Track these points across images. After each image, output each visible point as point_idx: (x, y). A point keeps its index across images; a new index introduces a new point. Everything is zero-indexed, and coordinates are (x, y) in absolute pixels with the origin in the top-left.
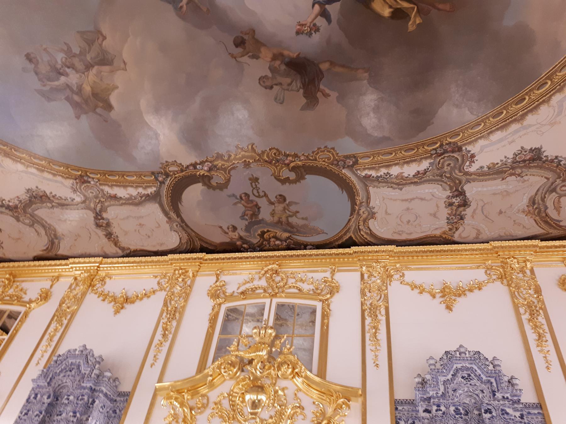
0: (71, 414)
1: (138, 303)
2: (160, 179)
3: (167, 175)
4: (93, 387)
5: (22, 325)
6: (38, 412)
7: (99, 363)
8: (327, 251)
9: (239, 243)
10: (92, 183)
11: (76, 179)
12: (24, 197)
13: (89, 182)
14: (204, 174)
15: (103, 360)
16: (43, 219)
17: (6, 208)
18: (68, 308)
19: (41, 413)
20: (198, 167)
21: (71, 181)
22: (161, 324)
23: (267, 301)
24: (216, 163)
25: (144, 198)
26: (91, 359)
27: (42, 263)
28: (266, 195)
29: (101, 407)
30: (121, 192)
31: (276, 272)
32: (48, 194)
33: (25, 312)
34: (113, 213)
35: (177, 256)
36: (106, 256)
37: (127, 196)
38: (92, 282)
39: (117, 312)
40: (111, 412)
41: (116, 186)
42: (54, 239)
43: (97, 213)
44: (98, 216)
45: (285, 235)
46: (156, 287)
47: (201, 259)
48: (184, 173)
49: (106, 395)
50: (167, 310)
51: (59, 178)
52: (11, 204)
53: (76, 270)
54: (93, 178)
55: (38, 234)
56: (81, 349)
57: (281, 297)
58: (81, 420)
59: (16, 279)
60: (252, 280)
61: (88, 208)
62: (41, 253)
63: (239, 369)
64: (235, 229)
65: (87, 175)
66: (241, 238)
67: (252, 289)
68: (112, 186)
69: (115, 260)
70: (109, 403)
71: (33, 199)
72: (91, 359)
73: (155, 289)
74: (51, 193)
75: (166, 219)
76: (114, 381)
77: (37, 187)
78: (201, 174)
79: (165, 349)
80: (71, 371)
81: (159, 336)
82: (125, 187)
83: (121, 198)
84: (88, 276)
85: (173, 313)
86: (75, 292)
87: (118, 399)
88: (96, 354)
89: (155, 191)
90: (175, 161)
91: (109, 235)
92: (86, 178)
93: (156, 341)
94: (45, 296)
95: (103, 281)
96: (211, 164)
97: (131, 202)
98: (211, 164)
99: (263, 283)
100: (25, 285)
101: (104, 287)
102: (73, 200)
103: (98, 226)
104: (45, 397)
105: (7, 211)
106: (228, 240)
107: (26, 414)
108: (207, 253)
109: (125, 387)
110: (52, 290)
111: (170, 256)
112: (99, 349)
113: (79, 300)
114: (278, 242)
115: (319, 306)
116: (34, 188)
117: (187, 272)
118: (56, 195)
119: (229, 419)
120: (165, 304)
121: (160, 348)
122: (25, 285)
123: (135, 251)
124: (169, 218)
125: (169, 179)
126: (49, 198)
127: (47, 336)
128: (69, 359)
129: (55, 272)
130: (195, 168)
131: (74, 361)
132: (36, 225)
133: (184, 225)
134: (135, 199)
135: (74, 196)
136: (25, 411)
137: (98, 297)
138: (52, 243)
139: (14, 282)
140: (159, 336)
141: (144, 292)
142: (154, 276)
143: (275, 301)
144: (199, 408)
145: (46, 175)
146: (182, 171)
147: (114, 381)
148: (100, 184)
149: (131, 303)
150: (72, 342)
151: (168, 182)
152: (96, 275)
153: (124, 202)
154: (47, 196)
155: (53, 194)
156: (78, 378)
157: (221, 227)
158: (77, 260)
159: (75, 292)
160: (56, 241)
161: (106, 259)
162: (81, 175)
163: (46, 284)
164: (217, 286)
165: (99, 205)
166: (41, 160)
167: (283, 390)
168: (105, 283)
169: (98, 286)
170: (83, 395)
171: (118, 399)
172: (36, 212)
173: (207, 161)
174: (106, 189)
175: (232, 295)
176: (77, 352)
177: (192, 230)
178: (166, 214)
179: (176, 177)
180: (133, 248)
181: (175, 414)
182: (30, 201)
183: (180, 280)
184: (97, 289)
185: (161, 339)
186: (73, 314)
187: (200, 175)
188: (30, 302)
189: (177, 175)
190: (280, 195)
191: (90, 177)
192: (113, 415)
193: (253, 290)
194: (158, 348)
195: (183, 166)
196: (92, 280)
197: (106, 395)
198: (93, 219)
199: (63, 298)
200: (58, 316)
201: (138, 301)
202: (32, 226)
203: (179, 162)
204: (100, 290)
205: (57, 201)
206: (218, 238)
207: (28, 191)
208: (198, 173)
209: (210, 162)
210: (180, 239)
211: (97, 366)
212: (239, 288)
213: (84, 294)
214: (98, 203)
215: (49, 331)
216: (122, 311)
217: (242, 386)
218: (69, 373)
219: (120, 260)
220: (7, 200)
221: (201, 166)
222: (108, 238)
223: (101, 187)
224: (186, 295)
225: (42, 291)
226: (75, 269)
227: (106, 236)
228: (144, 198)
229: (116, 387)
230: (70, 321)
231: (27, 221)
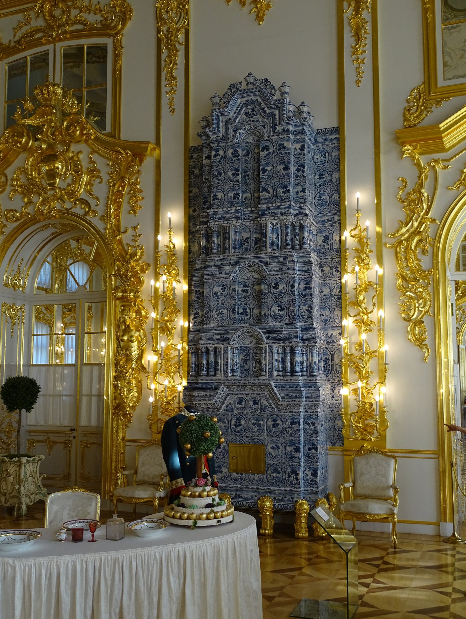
23: (50, 47)
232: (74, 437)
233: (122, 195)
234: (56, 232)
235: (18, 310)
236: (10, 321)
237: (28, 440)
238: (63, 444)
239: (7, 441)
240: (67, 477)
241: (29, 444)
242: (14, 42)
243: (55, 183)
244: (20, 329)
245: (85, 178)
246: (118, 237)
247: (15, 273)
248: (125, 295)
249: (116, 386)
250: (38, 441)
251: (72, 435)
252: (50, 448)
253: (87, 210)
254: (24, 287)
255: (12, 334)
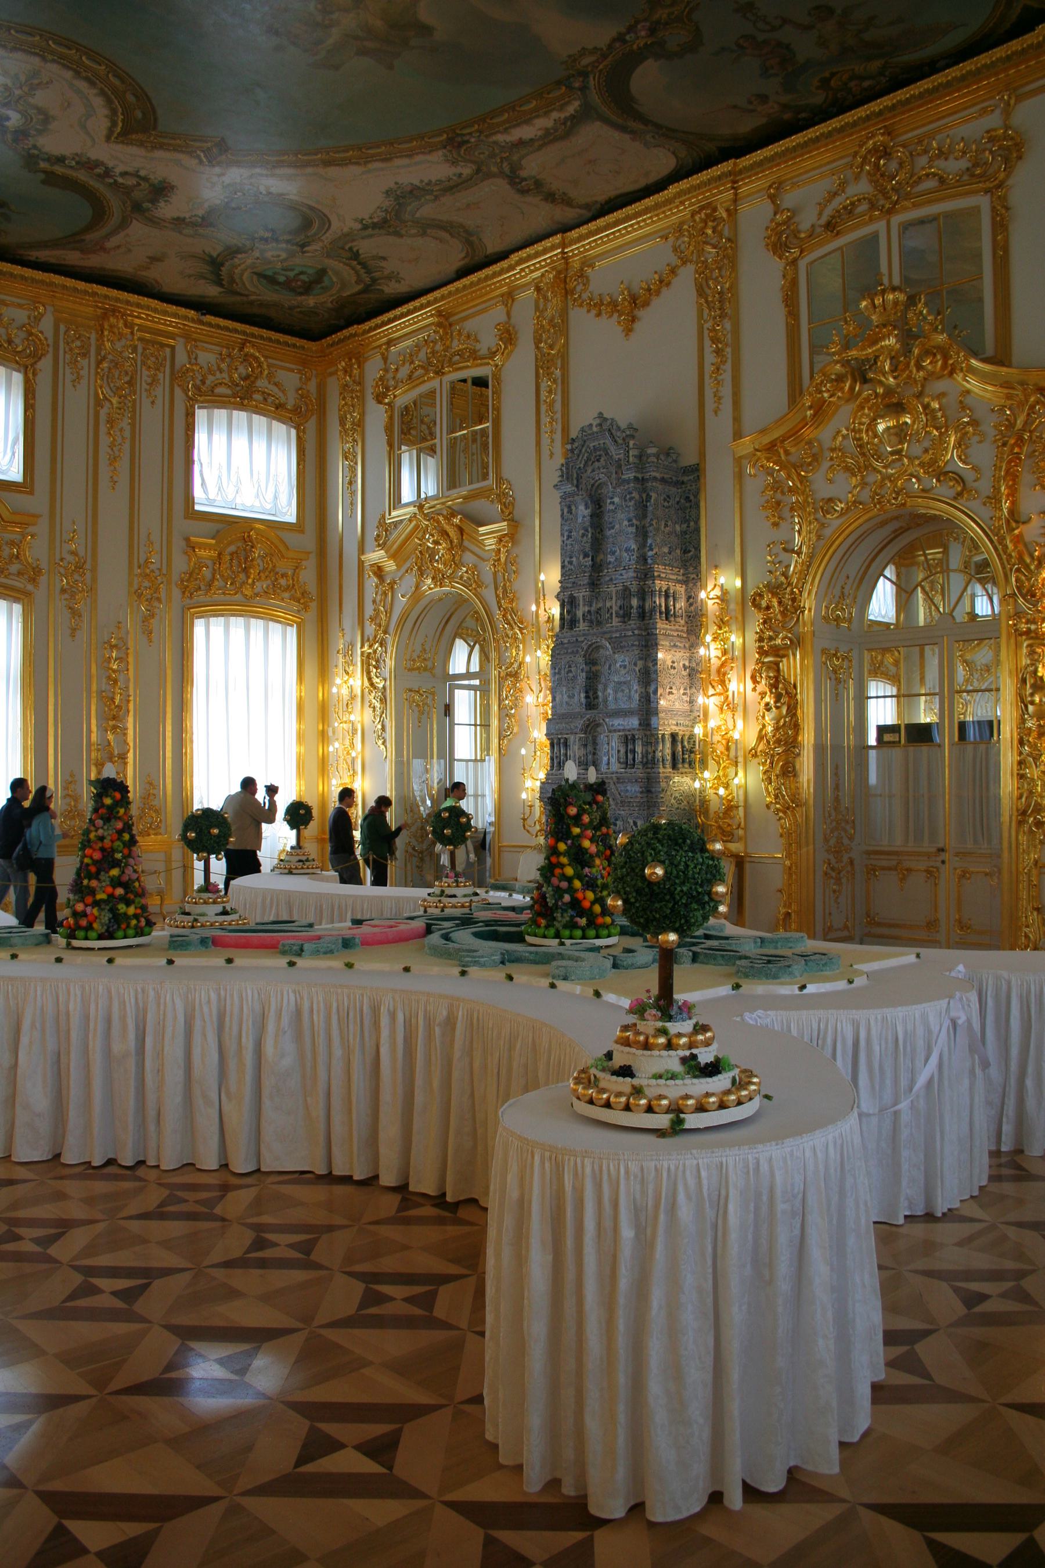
0: (626, 523)
1: (656, 302)
2: (577, 85)
3: (584, 74)
4: (640, 476)
5: (499, 397)
6: (582, 532)
7: (632, 437)
8: (983, 59)
9: (787, 116)
10: (473, 140)
11: (445, 148)
12: (387, 203)
13: (468, 142)
14: (646, 44)
15: (636, 430)
16: (433, 219)
17: (373, 228)
18: (551, 347)
19: (587, 531)
20: (628, 38)
21: (440, 153)
22: (706, 332)
23: (880, 226)
24: (656, 17)
25: (569, 123)
26: (619, 434)
27: (473, 278)
28: (785, 21)
29: (665, 500)
30: (526, 132)
31: (886, 153)
32: (418, 184)
33: (494, 375)
34: (532, 166)
35: (684, 184)
36: (566, 229)
37: (539, 133)
38: (566, 282)
39: (628, 331)
40: (682, 501)
41: (515, 126)
42: (468, 237)
43: (508, 176)
44: (514, 179)
45: (875, 65)
46: (675, 261)
47: (730, 173)
48: (610, 58)
49: (663, 480)
50: (707, 302)
51: (419, 158)
52: (375, 220)
53: (532, 272)
54: (470, 134)
55: (441, 241)
56: (598, 421)
57: (905, 209)
58: (644, 527)
59: (451, 319)
60: (843, 185)
61: (489, 175)
62: (462, 263)
63: (854, 381)
64: (763, 98)
65: (458, 135)
66: (785, 107)
67: (845, 208)
68: (506, 131)
69: (583, 230)
70: (674, 490)
71: (401, 201)
72: (619, 434)
73: (674, 265)
74: (422, 181)
75: (627, 137)
76: (668, 454)
77: (396, 183)
78: (641, 45)
79: (727, 376)
80: (598, 460)
81: (710, 358)
82: (528, 122)
83: (531, 140)
84: (555, 277)
85: (719, 304)
86: (549, 313)
87: (686, 479)
88: (623, 425)
89: (580, 106)
90: (583, 48)
91: (551, 197)
92: (459, 139)
93: (709, 369)
94: (508, 336)
95: (582, 276)
96: (648, 24)
97: (549, 138)
98: (648, 24)
99: (864, 187)
100: (470, 326)
101: (590, 289)
102: (460, 175)
103: (524, 192)
104: (582, 507)
105: (377, 231)
106: (764, 120)
107: (569, 537)
108: (737, 158)
109: (689, 459)
110: (513, 321)
111: (672, 190)
112: (623, 415)
113: (561, 326)
114: (866, 84)
115: (984, 202)
116: (392, 185)
117: (715, 210)
118: (430, 181)
119: (859, 471)
120: (701, 292)
121: (720, 378)
122: (470, 326)
123: (609, 201)
124: (632, 132)
125: (591, 78)
126: (423, 189)
127: (543, 408)
128: (587, 443)
129: (501, 287)
130: (625, 42)
131: (596, 443)
132: (429, 231)
133: (666, 133)
134: (556, 130)
135: (459, 170)
136: (566, 534)
137: (589, 311)
138: (469, 243)
139: (451, 325)
140: (710, 358)
141: (657, 277)
142: (661, 237)
143: (897, 220)
144: (810, 464)
145: (398, 162)
146: (604, 57)
147: (668, 454)
148: (487, 136)
149: (643, 306)
150: (583, 416)
151: (592, 82)
152: (567, 269)
153: (541, 142)
154: (419, 188)
155: (426, 181)
156: (613, 469)
157: (735, 107)
158: (523, 254)
159: (549, 313)
160: (474, 238)
161: (568, 234)
162: (448, 138)
163: (498, 313)
164: (778, 225)
165: (505, 164)
166: (378, 147)
167: (940, 396)
168: (587, 277)
169: (579, 288)
170: (630, 493)
171: (686, 479)
172: (418, 215)
173: (637, 22)
174: (500, 138)
175: (811, 235)
176: (595, 429)
177: (684, 132)
178: (623, 129)
179: (601, 71)
180: (601, 198)
181: (775, 481)
182: (399, 204)
183: (709, 232)
184: (580, 296)
185: (714, 360)
186: (564, 356)
187: (639, 48)
188: (492, 354)
189: (601, 67)
190: (818, 8)
191: (464, 135)
192: (688, 505)
193: (849, 210)
194: (716, 379)
195: (602, 49)
196: (565, 282)
197: (663, 480)
198: (508, 187)
199: (536, 332)
200: (543, 365)
201: (653, 298)
202: (424, 234)
203: (590, 47)
204: (585, 296)
205: (438, 188)
206: (746, 126)
207: (388, 193)
208: (635, 47)
209: (645, 20)
210: (674, 153)
211: (631, 443)
212: (820, 214)
213: (564, 313)
214: (502, 162)
215: (543, 398)
216: (637, 326)
217: (869, 409)
218: (597, 464)
219: (592, 226)
220: (366, 217)
221: (632, 35)
222: (552, 202)
223: (491, 140)
224: (730, 258)
225: (499, 330)
226: (531, 269)
227: (546, 199)
228: (569, 123)
229: (675, 461)
230: (565, 369)
231: (414, 231)
232: (943, 862)
233: (1020, 459)
234: (901, 527)
235: (843, 660)
236: (833, 677)
237: (866, 866)
238: (925, 874)
239: (836, 866)
240: (932, 925)
241: (868, 873)
242: (821, 226)
243: (902, 450)
244: (848, 689)
245: (953, 439)
246: (1016, 532)
247: (837, 599)
248: (1033, 627)
249: (1021, 777)
250: (883, 868)
251: (940, 859)
252: (903, 879)
253: (959, 489)
254: (850, 620)
255: (837, 697)
